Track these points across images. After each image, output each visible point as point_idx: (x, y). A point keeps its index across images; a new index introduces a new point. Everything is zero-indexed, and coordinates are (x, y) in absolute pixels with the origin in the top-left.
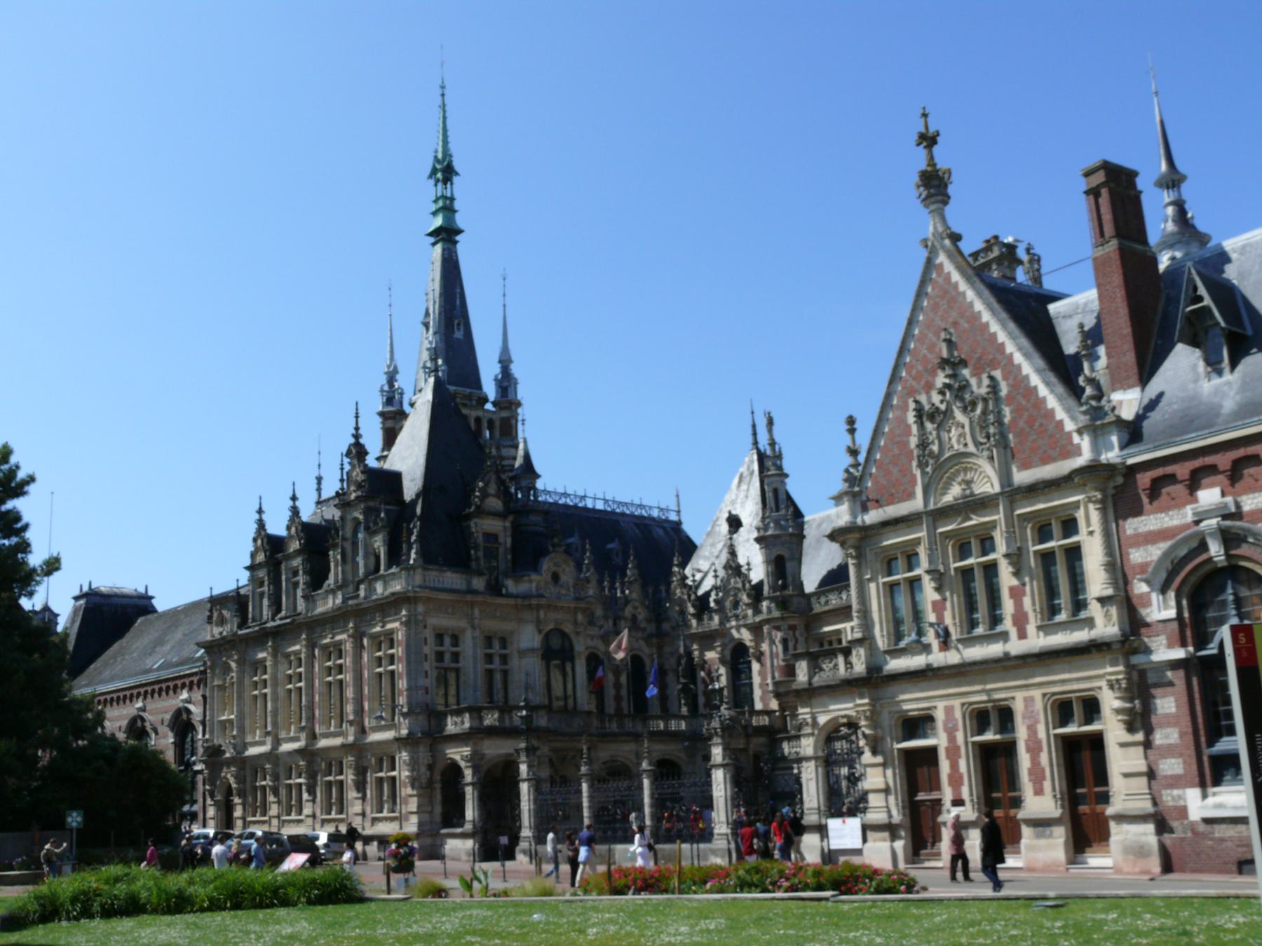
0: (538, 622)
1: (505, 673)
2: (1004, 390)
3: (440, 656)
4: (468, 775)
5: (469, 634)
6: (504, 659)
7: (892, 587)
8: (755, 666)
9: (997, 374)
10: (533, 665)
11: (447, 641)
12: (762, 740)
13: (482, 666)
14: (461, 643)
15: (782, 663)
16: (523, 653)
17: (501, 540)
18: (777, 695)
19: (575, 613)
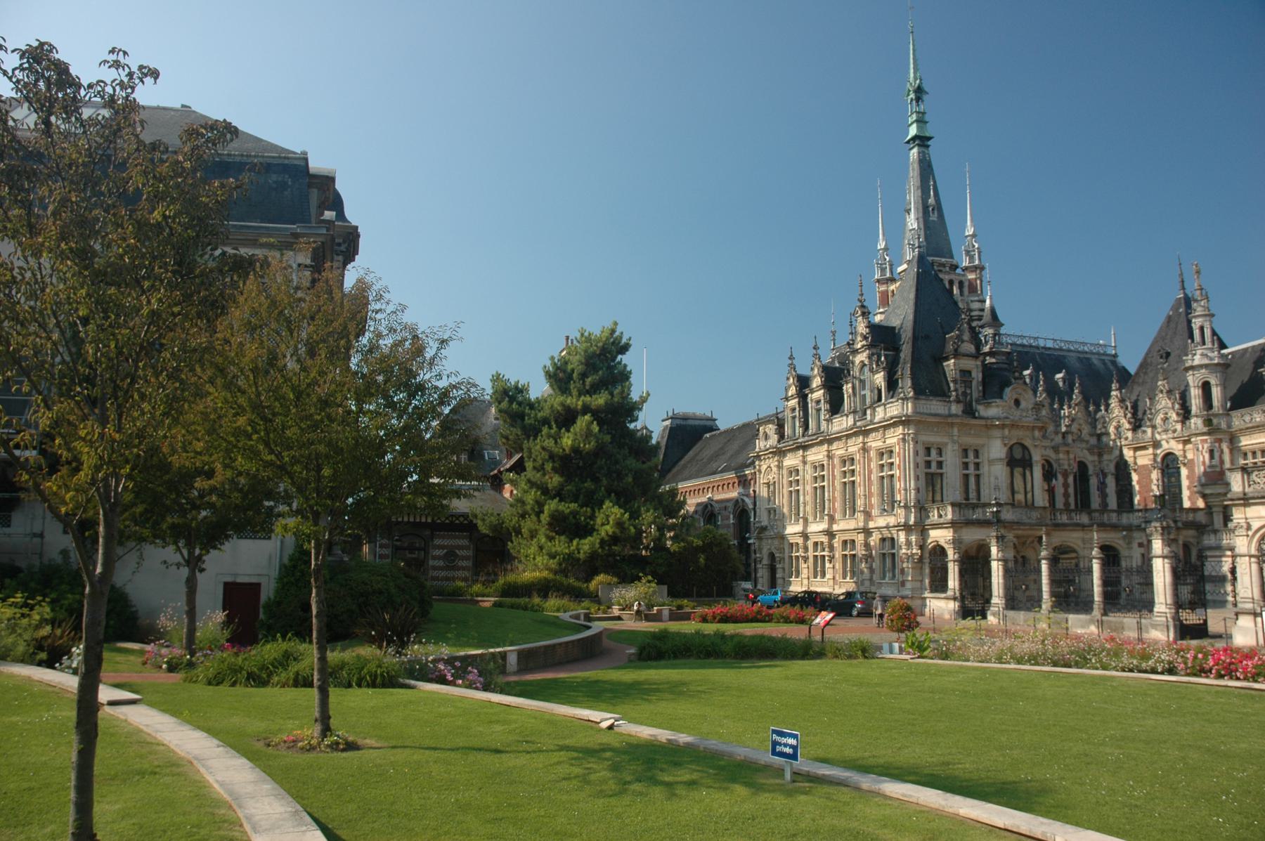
0: (1003, 438)
1: (978, 477)
3: (928, 464)
4: (951, 554)
5: (949, 447)
6: (977, 466)
8: (1184, 472)
12: (1192, 532)
16: (991, 462)
17: (974, 374)
18: (1204, 496)
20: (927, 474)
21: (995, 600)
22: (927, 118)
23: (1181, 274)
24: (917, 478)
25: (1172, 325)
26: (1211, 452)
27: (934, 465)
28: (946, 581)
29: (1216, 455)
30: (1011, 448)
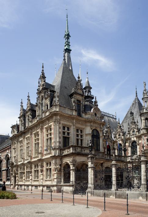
0: (91, 126)
3: (64, 133)
4: (72, 167)
5: (72, 127)
6: (81, 136)
10: (89, 138)
11: (66, 129)
13: (75, 137)
15: (146, 145)
16: (86, 135)
17: (81, 102)
19: (100, 125)
20: (63, 137)
21: (89, 185)
22: (70, 44)
23: (136, 92)
24: (60, 138)
25: (134, 106)
27: (66, 133)
28: (70, 178)
30: (93, 131)
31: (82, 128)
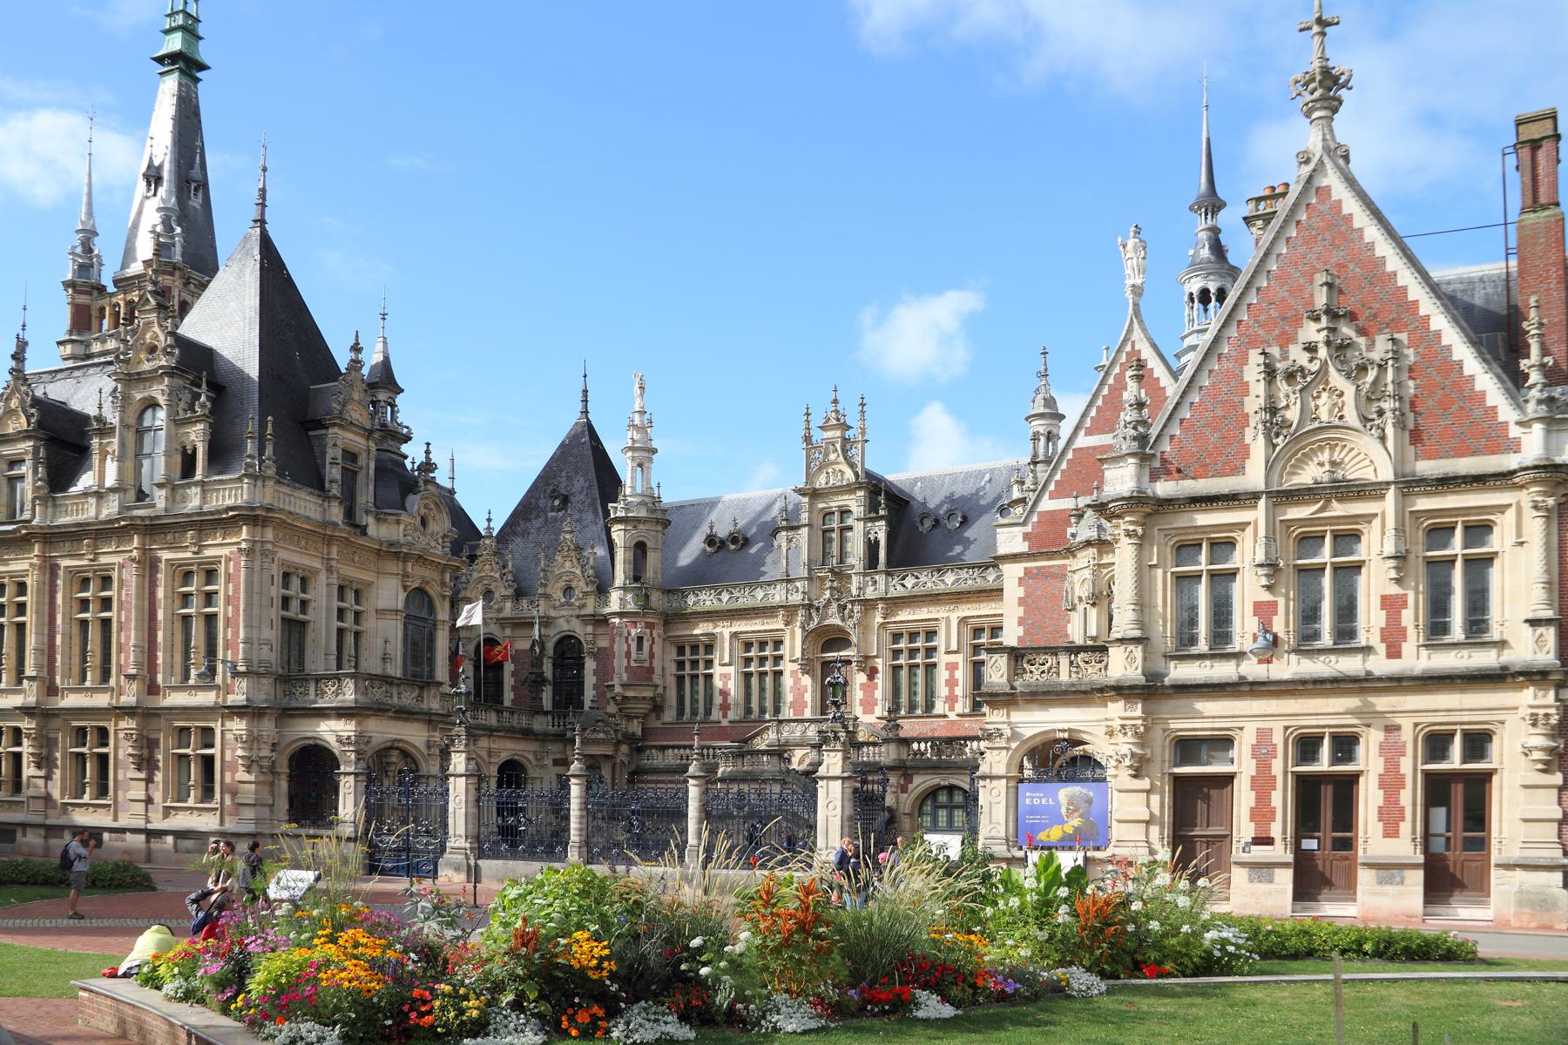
0: (405, 575)
1: (357, 635)
2: (1411, 355)
3: (286, 601)
5: (323, 577)
6: (357, 614)
7: (1180, 578)
8: (590, 664)
9: (1403, 337)
11: (295, 583)
14: (310, 587)
19: (443, 572)
20: (284, 619)
26: (640, 639)
27: (295, 605)
29: (646, 645)
31: (362, 582)
